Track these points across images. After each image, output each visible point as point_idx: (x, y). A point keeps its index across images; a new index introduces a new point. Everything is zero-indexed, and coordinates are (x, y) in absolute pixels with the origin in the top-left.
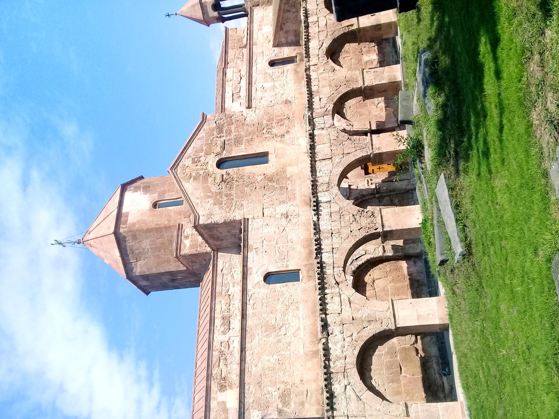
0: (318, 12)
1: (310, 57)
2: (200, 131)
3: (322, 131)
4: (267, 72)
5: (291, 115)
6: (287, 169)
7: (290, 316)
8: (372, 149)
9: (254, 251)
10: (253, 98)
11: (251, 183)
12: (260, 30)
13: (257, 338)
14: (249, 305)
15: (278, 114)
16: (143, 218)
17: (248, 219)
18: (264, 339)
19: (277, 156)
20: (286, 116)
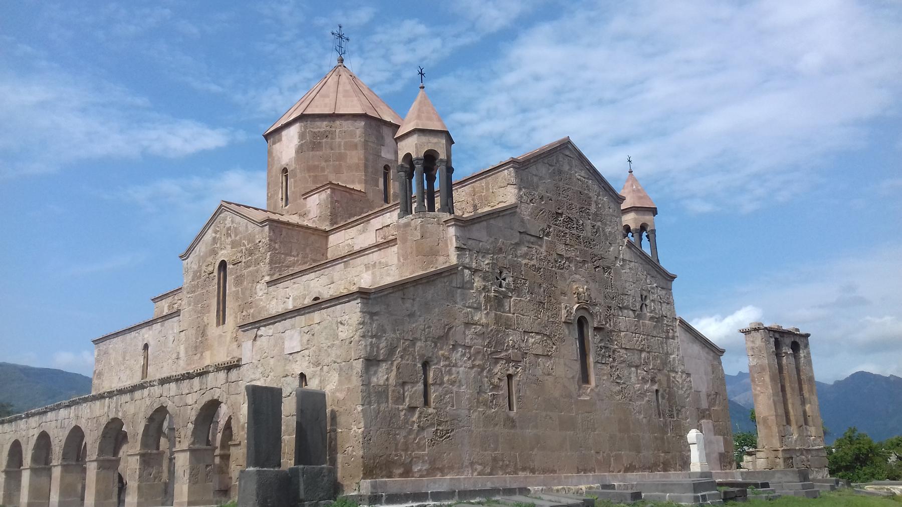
1: (162, 385)
7: (128, 372)
12: (366, 268)
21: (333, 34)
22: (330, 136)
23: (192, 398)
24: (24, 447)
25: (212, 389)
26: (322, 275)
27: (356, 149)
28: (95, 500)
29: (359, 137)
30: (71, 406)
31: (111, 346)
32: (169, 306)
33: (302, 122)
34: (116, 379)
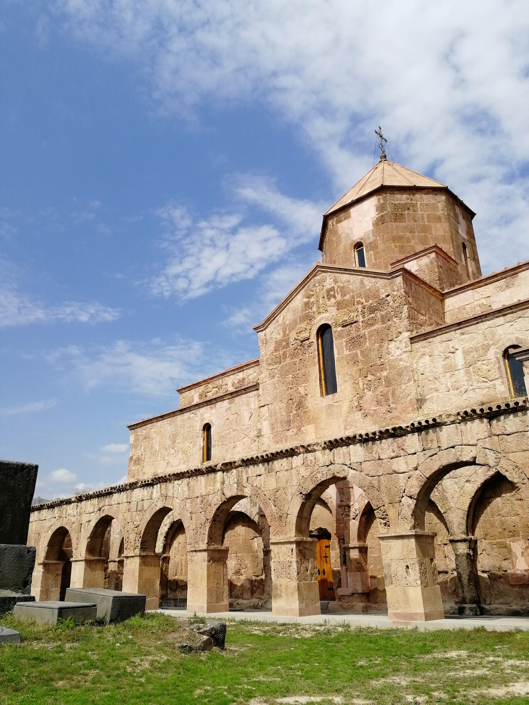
0: (429, 453)
1: (331, 450)
2: (374, 277)
3: (219, 483)
4: (491, 349)
5: (395, 413)
6: (311, 425)
7: (180, 456)
8: (192, 551)
9: (229, 406)
10: (430, 340)
11: (297, 381)
13: (169, 428)
14: (190, 414)
15: (397, 393)
16: (343, 240)
17: (258, 389)
18: (168, 436)
19: (330, 406)
20: (394, 405)
21: (376, 132)
22: (411, 208)
23: (407, 463)
24: (73, 535)
25: (453, 447)
26: (520, 317)
27: (440, 222)
28: (208, 603)
29: (442, 210)
30: (155, 484)
31: (153, 430)
32: (201, 396)
33: (380, 195)
34: (163, 464)
